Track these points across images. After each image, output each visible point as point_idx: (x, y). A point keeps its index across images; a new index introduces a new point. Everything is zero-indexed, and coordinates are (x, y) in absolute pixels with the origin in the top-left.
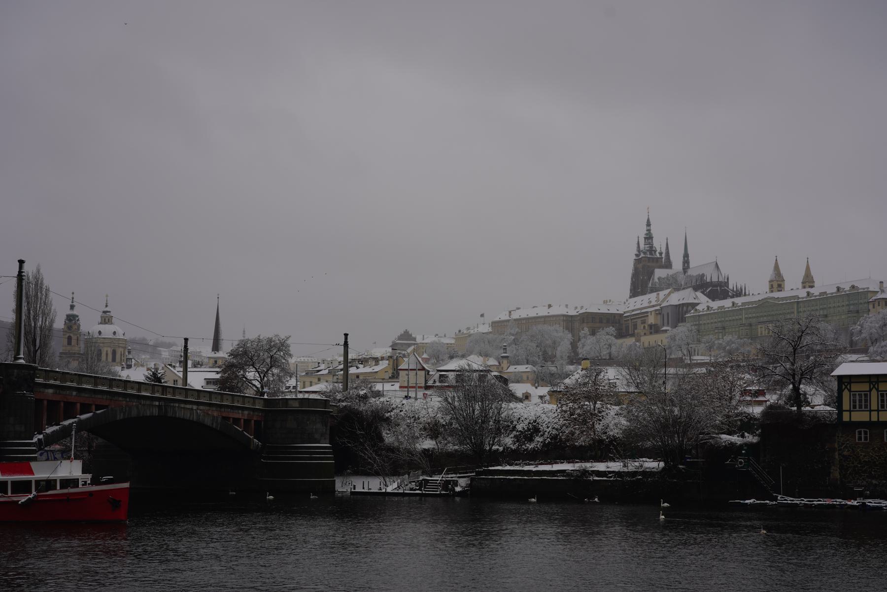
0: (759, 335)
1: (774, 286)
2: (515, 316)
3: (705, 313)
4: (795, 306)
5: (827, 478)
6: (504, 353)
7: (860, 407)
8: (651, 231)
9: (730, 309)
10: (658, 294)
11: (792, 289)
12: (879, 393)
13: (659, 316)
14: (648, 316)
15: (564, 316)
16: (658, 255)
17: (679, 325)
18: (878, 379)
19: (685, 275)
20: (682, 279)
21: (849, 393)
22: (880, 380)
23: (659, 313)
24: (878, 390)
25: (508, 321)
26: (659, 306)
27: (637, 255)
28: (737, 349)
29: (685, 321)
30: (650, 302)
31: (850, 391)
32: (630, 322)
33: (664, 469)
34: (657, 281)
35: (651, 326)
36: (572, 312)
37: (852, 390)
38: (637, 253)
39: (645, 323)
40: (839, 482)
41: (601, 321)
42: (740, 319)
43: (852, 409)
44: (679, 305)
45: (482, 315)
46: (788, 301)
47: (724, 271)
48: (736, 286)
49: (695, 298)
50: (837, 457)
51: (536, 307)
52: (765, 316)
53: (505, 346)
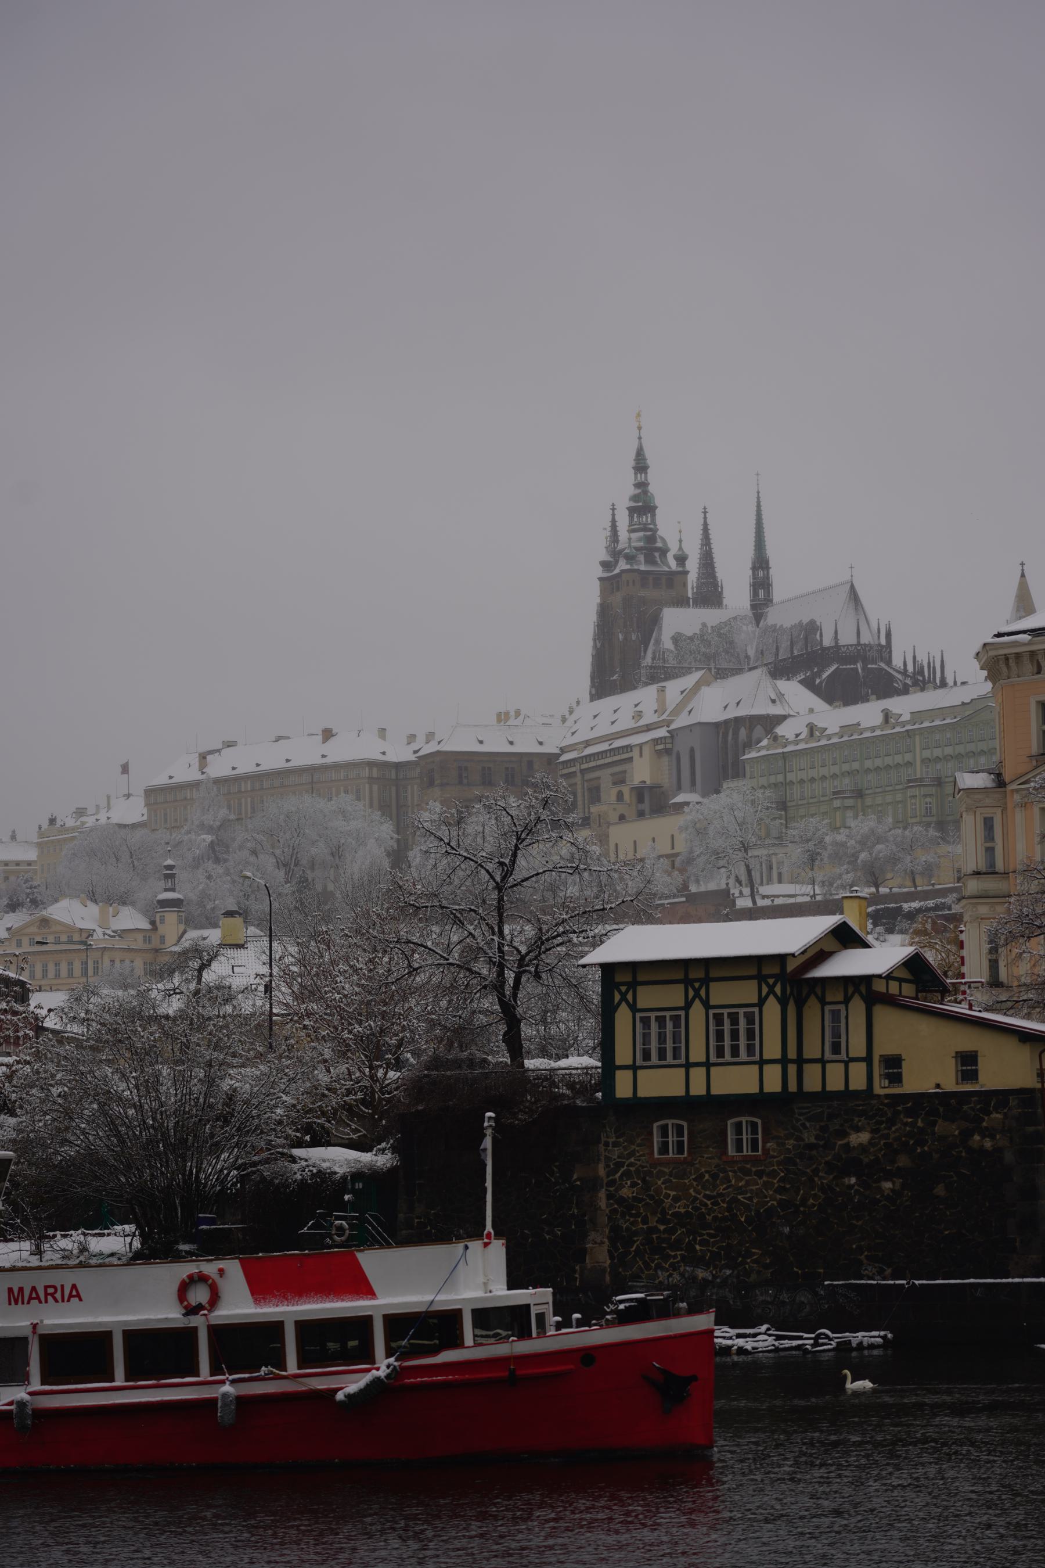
2: (219, 767)
3: (802, 746)
5: (577, 1268)
6: (166, 890)
8: (651, 488)
9: (878, 733)
10: (662, 690)
12: (711, 1012)
13: (665, 759)
14: (630, 759)
15: (371, 764)
16: (673, 564)
17: (725, 785)
18: (707, 973)
21: (630, 1014)
23: (665, 749)
25: (195, 785)
26: (665, 729)
27: (606, 565)
28: (894, 860)
29: (745, 776)
30: (639, 715)
31: (633, 1008)
32: (578, 779)
34: (668, 644)
35: (640, 793)
36: (399, 753)
37: (639, 1006)
38: (608, 558)
39: (623, 782)
40: (608, 1278)
42: (909, 764)
43: (639, 1062)
44: (726, 722)
45: (125, 769)
47: (877, 611)
48: (914, 658)
49: (773, 701)
50: (603, 1204)
51: (288, 738)
53: (170, 867)
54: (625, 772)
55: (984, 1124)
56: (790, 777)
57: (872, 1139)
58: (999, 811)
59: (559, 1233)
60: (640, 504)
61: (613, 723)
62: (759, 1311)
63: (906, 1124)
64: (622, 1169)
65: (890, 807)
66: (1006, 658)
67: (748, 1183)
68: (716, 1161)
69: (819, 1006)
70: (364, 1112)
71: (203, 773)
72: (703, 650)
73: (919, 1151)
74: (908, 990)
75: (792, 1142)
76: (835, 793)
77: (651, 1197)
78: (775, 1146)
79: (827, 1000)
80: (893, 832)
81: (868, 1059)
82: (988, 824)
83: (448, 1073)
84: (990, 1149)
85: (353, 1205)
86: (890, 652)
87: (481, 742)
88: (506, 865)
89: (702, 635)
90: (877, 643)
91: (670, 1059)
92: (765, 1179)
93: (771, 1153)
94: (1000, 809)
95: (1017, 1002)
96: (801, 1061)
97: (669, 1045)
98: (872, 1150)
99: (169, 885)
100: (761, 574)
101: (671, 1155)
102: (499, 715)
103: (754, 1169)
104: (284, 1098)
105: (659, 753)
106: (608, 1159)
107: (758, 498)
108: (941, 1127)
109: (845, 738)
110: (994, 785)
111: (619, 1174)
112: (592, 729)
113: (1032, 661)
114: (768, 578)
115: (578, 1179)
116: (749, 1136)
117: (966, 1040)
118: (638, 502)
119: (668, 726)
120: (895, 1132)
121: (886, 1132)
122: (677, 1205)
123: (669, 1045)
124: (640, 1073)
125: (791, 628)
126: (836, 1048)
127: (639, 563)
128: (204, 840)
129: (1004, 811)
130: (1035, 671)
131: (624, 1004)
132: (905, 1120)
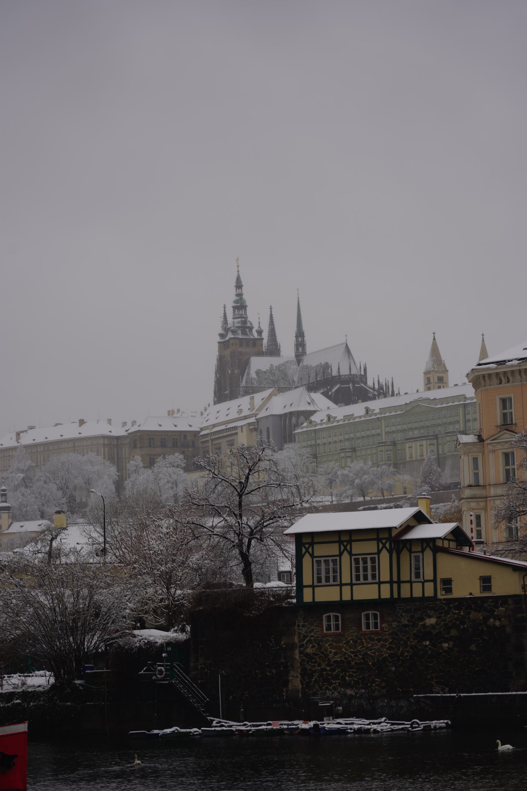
0: (408, 459)
1: (432, 381)
2: (26, 440)
3: (324, 426)
4: (461, 410)
5: (284, 690)
6: (2, 502)
7: (327, 579)
8: (244, 297)
9: (363, 419)
10: (252, 398)
11: (456, 385)
12: (353, 557)
13: (254, 433)
14: (237, 433)
15: (104, 437)
16: (256, 335)
17: (285, 446)
18: (350, 538)
19: (299, 365)
20: (294, 372)
22: (316, 540)
23: (254, 428)
24: (350, 554)
25: (14, 449)
26: (254, 418)
27: (221, 336)
28: (372, 483)
29: (295, 441)
30: (241, 411)
31: (312, 556)
32: (210, 444)
33: (53, 686)
34: (253, 375)
36: (118, 431)
37: (315, 555)
38: (223, 332)
40: (300, 695)
41: (163, 445)
42: (379, 435)
43: (316, 584)
46: (450, 404)
48: (379, 381)
49: (309, 404)
50: (297, 657)
51: (61, 424)
52: (416, 428)
53: (4, 490)
54: (234, 440)
55: (496, 613)
56: (318, 441)
57: (437, 621)
58: (480, 454)
59: (275, 672)
60: (239, 305)
61: (227, 415)
62: (380, 711)
63: (455, 614)
64: (307, 639)
65: (369, 456)
66: (484, 376)
67: (373, 645)
68: (356, 634)
69: (408, 553)
70: (164, 611)
71: (18, 442)
72: (271, 378)
73: (462, 627)
74: (453, 545)
75: (395, 623)
76: (341, 450)
77: (323, 653)
78: (387, 626)
79: (413, 550)
80: (372, 469)
81: (434, 581)
82: (475, 460)
83: (215, 590)
84: (499, 626)
85: (167, 659)
86: (366, 378)
87: (160, 426)
88: (243, 483)
89: (271, 371)
90: (359, 374)
91: (331, 582)
92: (382, 643)
93: (385, 629)
94: (481, 453)
95: (506, 550)
96: (399, 582)
97: (331, 575)
98: (437, 627)
99: (4, 499)
100: (300, 339)
101: (332, 631)
102: (169, 412)
103: (376, 638)
104: (129, 605)
105: (251, 430)
106: (300, 633)
107: (298, 301)
108: (473, 615)
109: (346, 422)
110: (478, 441)
111: (305, 641)
112: (216, 418)
113: (497, 378)
114: (304, 341)
115: (284, 644)
116: (373, 621)
117: (485, 570)
118: (238, 304)
119: (256, 417)
120: (449, 618)
121: (444, 618)
122: (336, 657)
123: (331, 575)
124: (316, 589)
125: (316, 366)
126: (418, 575)
127: (238, 334)
128: (20, 476)
129: (483, 454)
130: (499, 383)
131: (307, 554)
132: (454, 612)
